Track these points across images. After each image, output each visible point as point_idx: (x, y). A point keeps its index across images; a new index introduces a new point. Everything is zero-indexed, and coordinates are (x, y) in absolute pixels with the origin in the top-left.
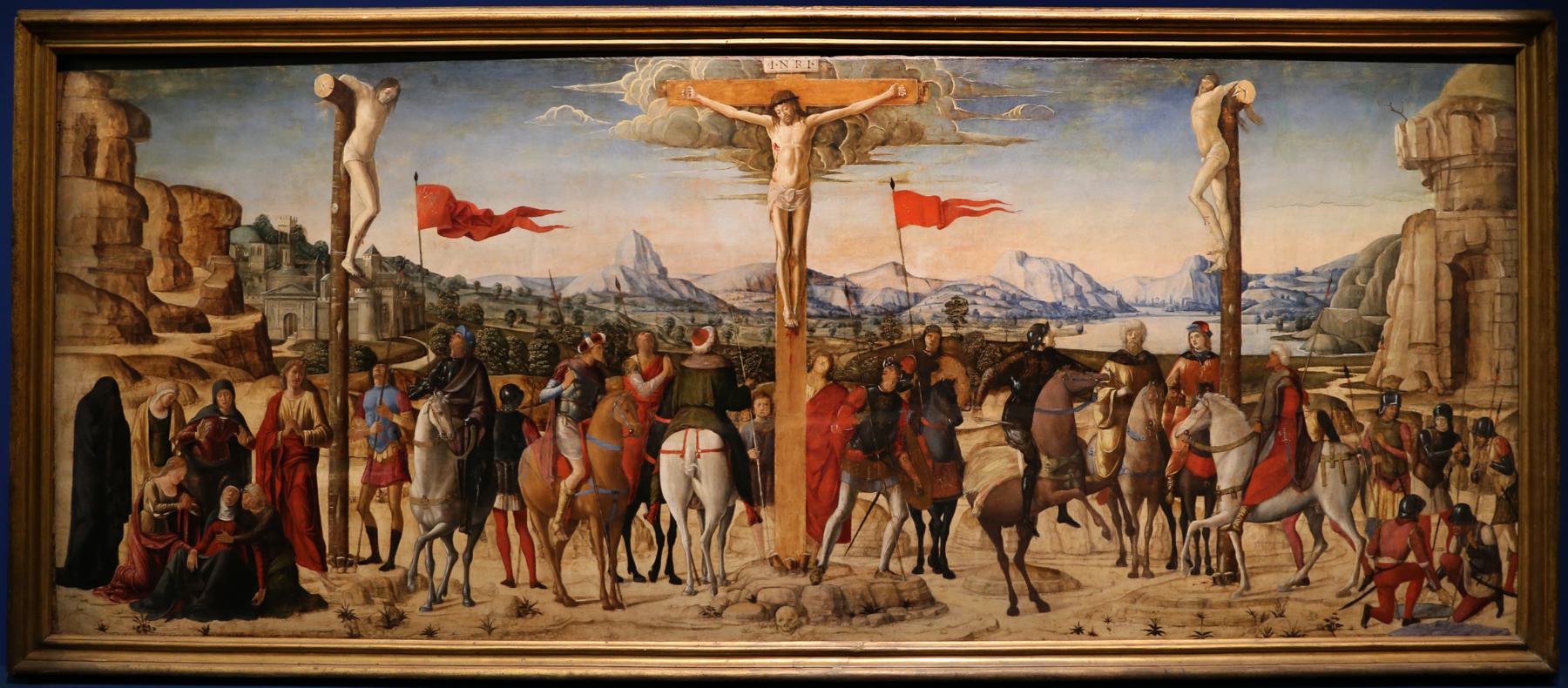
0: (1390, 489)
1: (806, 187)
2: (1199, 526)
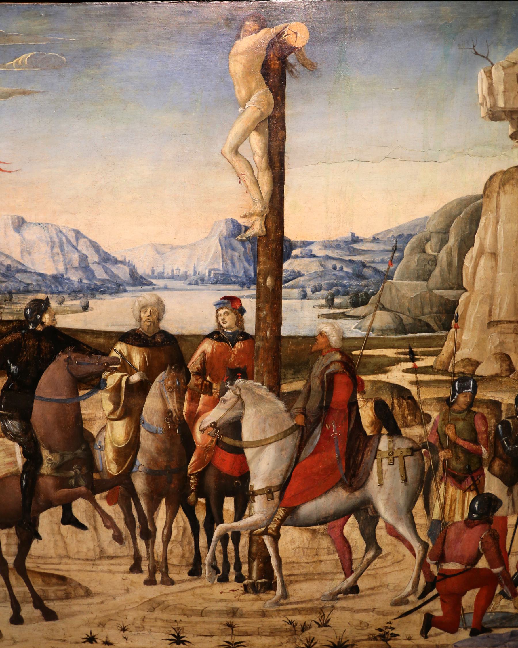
0: (460, 488)
2: (227, 530)
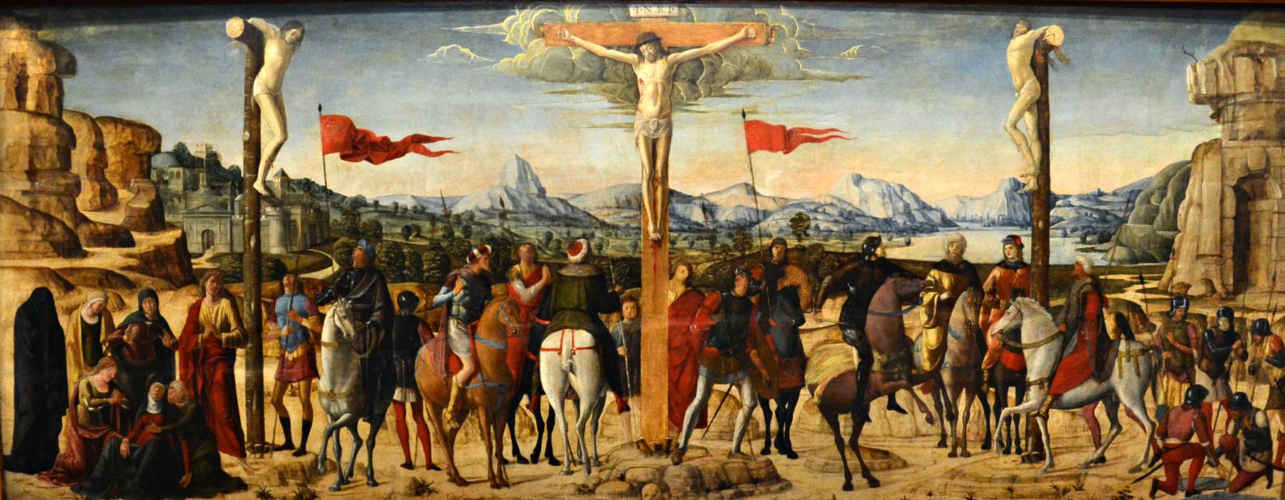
1: (668, 117)
2: (1010, 412)
